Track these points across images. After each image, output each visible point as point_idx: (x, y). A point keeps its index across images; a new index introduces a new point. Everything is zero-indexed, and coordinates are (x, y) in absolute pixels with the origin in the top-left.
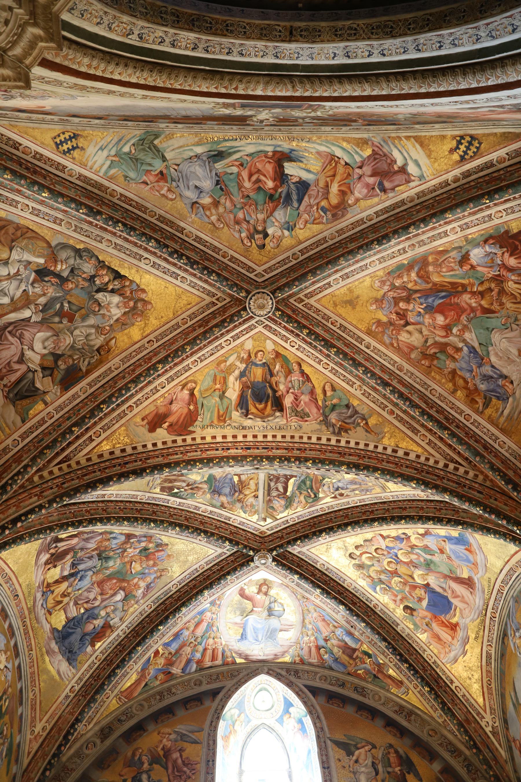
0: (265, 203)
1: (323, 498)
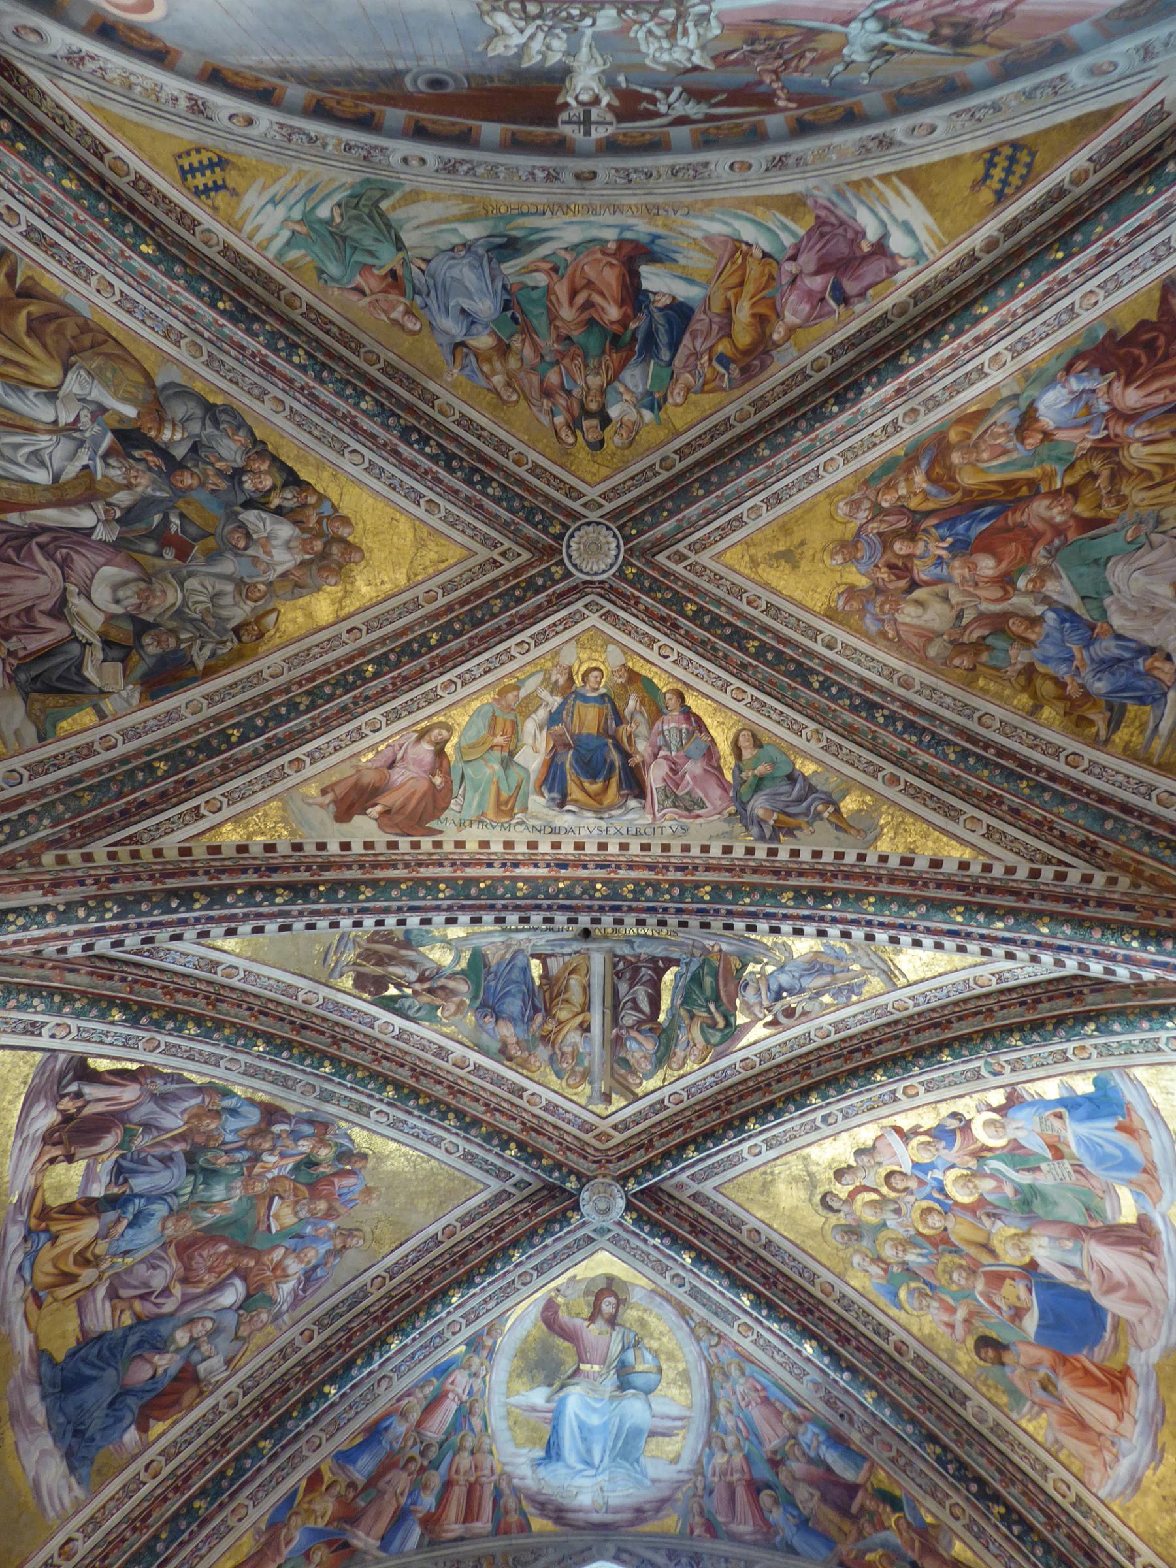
0: (603, 352)
1: (747, 1027)
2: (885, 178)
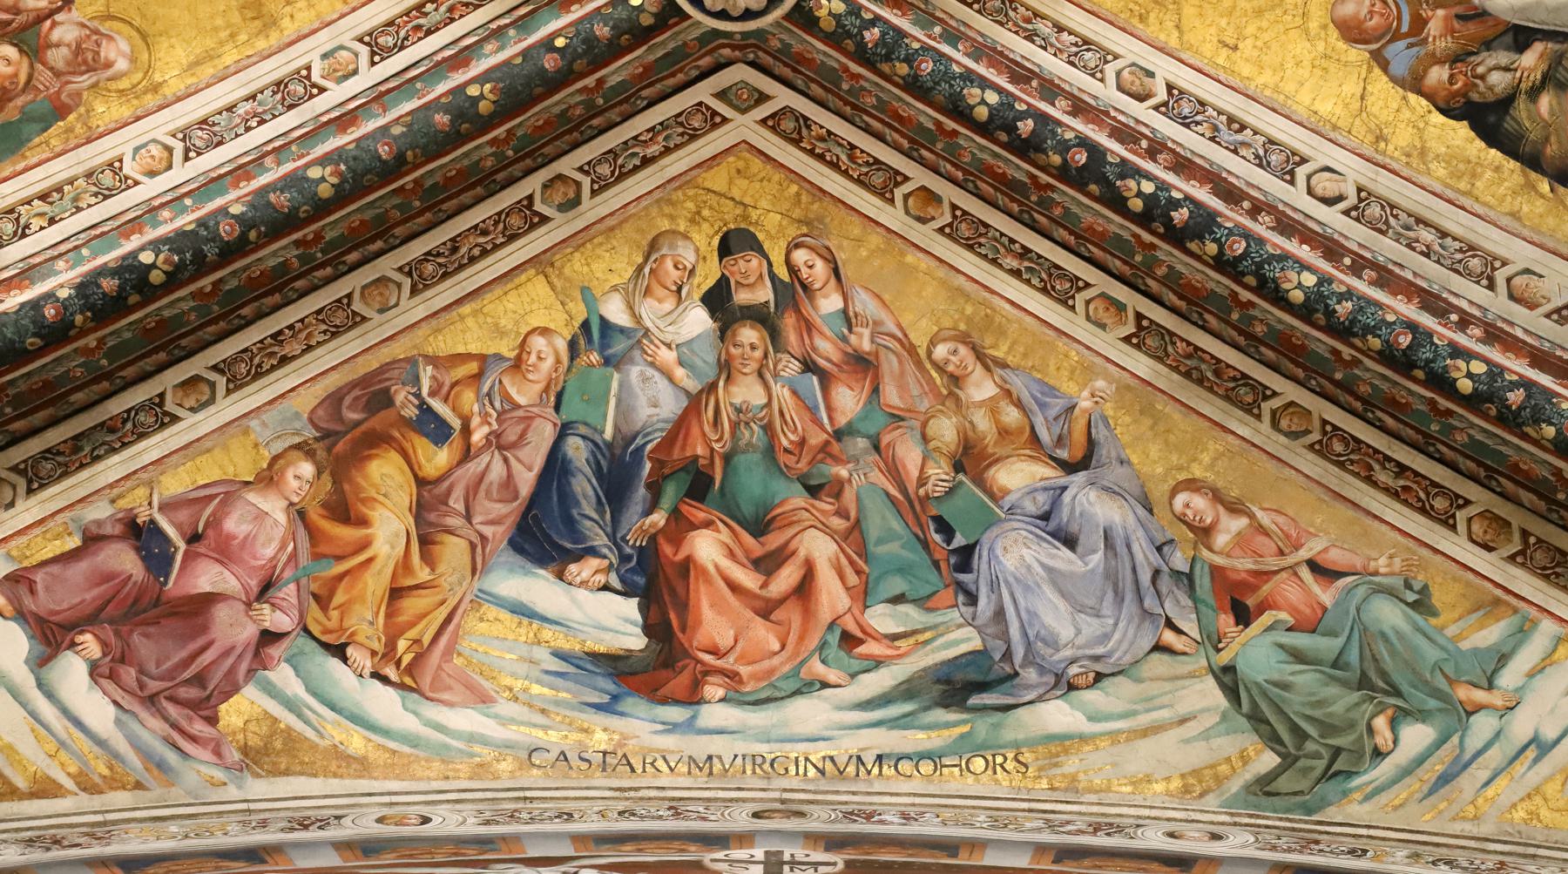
0: (727, 459)
2: (45, 789)
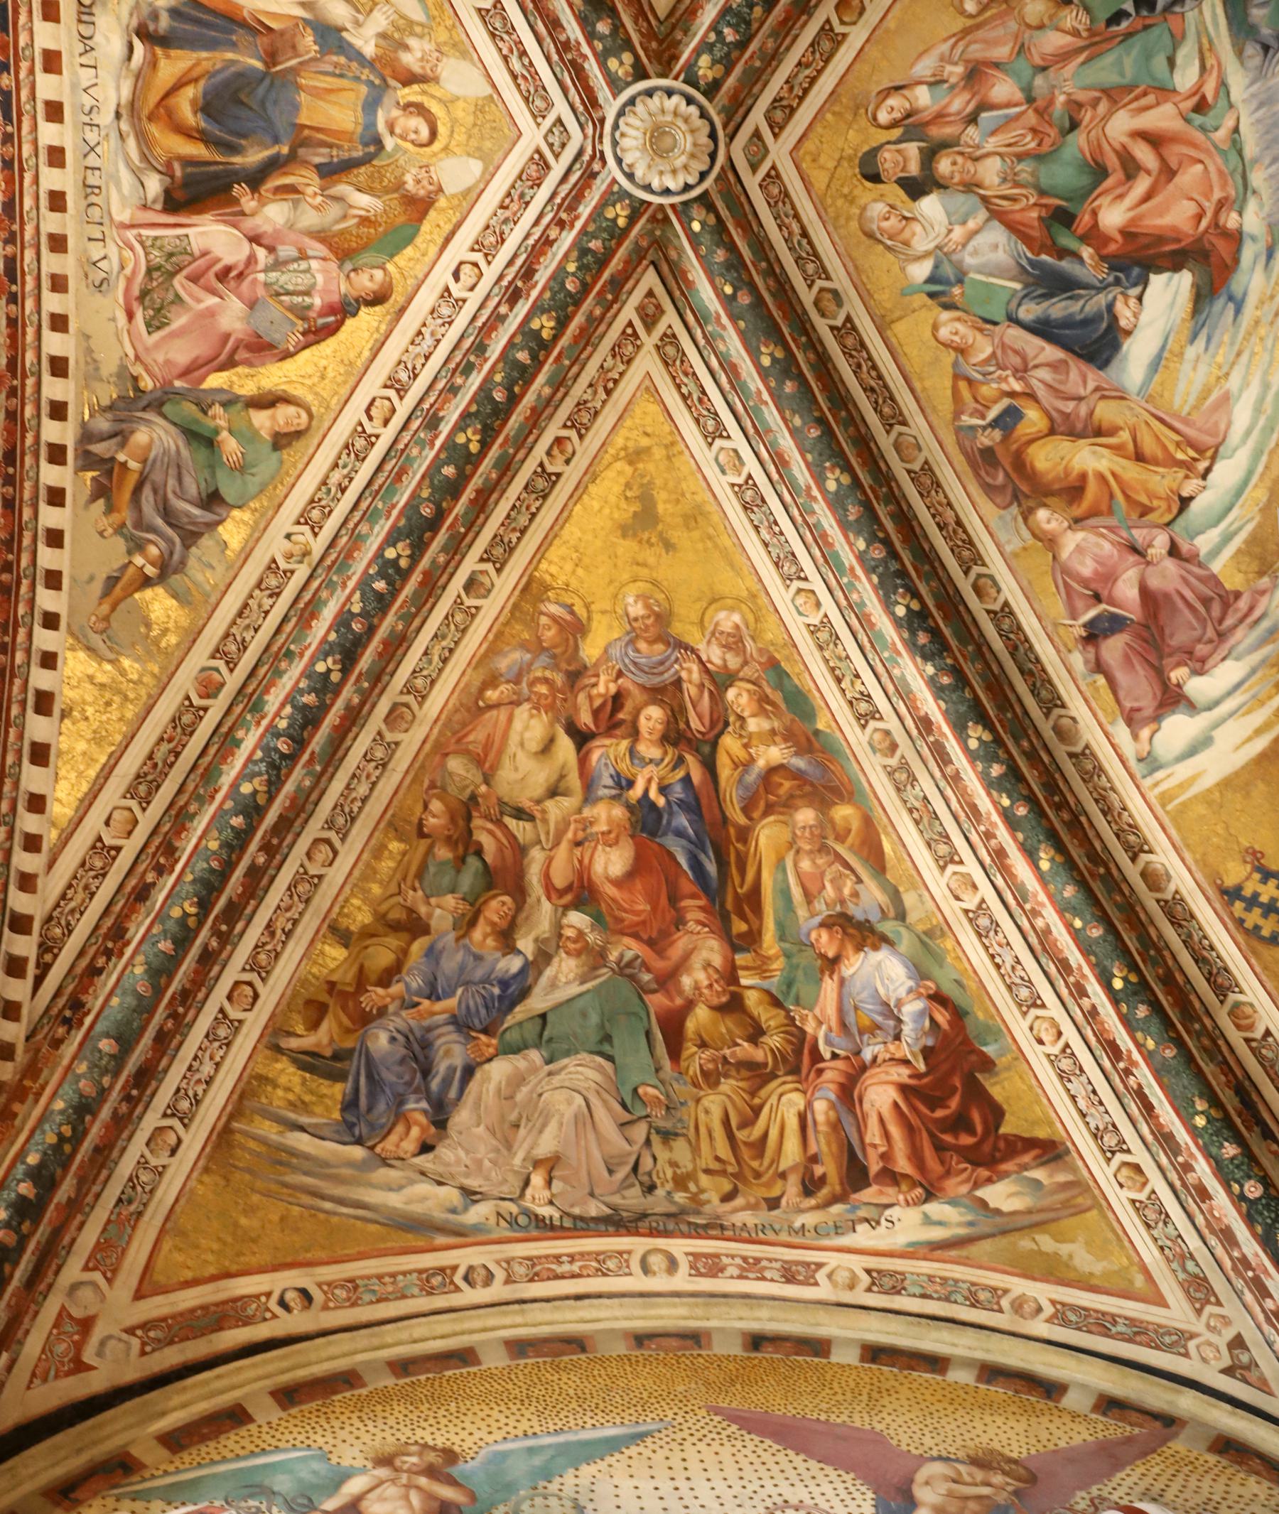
0: (1042, 193)
